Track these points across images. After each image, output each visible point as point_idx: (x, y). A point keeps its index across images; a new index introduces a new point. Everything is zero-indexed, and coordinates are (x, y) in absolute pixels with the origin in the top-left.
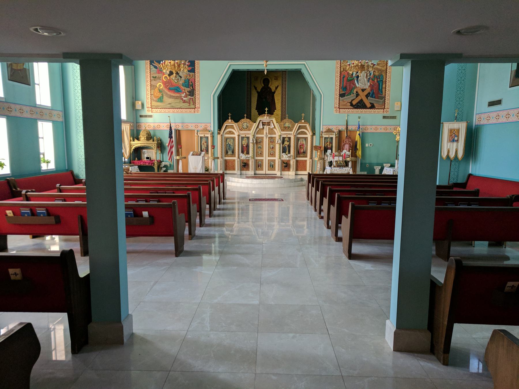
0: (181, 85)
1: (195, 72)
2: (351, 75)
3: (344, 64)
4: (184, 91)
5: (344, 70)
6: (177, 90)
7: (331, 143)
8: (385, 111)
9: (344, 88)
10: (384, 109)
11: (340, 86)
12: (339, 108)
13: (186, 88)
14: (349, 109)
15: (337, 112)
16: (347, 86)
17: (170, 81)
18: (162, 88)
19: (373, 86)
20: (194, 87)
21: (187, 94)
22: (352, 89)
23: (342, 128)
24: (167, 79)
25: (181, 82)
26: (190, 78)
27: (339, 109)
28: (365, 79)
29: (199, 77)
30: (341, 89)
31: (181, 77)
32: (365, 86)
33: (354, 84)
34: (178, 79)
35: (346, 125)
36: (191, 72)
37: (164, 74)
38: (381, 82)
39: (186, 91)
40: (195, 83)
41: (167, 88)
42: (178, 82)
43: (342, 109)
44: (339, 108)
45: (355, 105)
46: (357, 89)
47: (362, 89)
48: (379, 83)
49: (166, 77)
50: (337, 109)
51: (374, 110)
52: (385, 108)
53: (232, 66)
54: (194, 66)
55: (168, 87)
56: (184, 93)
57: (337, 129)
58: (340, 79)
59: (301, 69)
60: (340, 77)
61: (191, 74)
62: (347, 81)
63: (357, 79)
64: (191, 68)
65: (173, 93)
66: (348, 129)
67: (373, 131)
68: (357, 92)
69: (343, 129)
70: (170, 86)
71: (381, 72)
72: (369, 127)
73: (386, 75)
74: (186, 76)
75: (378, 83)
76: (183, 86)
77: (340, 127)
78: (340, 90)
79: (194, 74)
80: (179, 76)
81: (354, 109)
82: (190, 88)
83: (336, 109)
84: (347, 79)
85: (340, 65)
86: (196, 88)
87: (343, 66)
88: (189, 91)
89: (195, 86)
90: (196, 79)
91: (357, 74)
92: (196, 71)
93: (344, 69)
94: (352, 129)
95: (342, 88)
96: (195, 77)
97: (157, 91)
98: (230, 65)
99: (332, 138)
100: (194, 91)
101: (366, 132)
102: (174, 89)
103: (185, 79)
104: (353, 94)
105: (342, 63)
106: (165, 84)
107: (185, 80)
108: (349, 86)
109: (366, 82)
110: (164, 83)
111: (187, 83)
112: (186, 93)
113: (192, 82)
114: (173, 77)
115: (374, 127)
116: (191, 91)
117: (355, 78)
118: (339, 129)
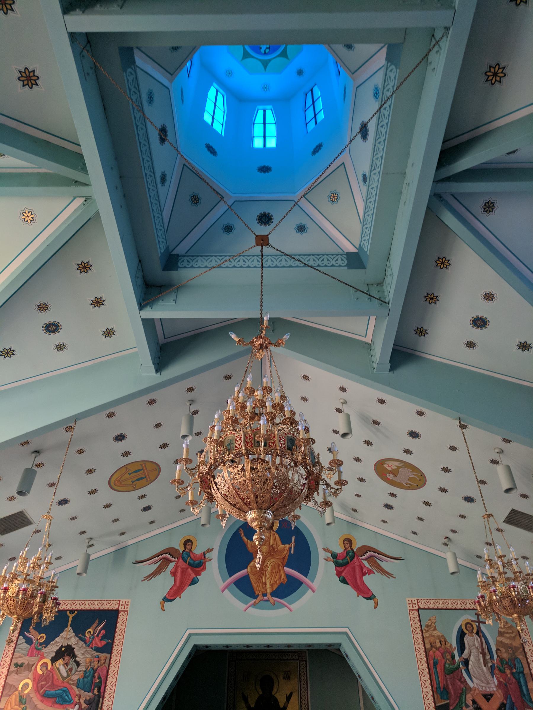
0: (73, 684)
1: (111, 653)
2: (451, 659)
3: (430, 632)
4: (77, 699)
5: (432, 646)
6: (60, 696)
9: (442, 692)
11: (431, 684)
13: (83, 691)
16: (447, 684)
17: (51, 675)
18: (28, 694)
19: (506, 686)
20: (102, 690)
21: (83, 707)
22: (462, 694)
24: (47, 668)
25: (75, 677)
26: (98, 667)
28: (484, 668)
29: (118, 663)
30: (437, 693)
31: (78, 664)
32: (489, 686)
33: (462, 680)
34: (71, 670)
36: (103, 653)
37: (42, 657)
38: (521, 675)
39: (82, 701)
40: (107, 680)
41: (39, 692)
42: (68, 676)
46: (472, 692)
47: (483, 693)
48: (518, 677)
49: (45, 664)
53: (192, 637)
54: (114, 637)
55: (42, 690)
56: (77, 706)
58: (428, 667)
59: (340, 645)
60: (427, 662)
61: (103, 655)
62: (445, 674)
63: (465, 668)
64: (104, 642)
65: (51, 706)
68: (474, 702)
70: (48, 687)
71: (514, 653)
73: (527, 659)
74: (91, 663)
75: (515, 678)
76: (78, 687)
78: (433, 695)
79: (108, 655)
80: (75, 661)
82: (93, 693)
84: (445, 668)
85: (422, 635)
86: (108, 691)
87: (427, 637)
88: (89, 700)
89: (106, 685)
90: (112, 668)
91: (463, 656)
92: (113, 651)
93: (432, 644)
95: (439, 692)
96: (110, 663)
97: (15, 700)
98: (190, 636)
100: (101, 699)
102: (56, 694)
103: (86, 669)
104: (467, 706)
105: (424, 631)
106: (38, 683)
107: (85, 672)
108: (453, 684)
109: (487, 675)
110: (37, 680)
111: (89, 678)
112: (79, 704)
113: (99, 677)
114: (60, 665)
116: (94, 698)
117: (461, 666)
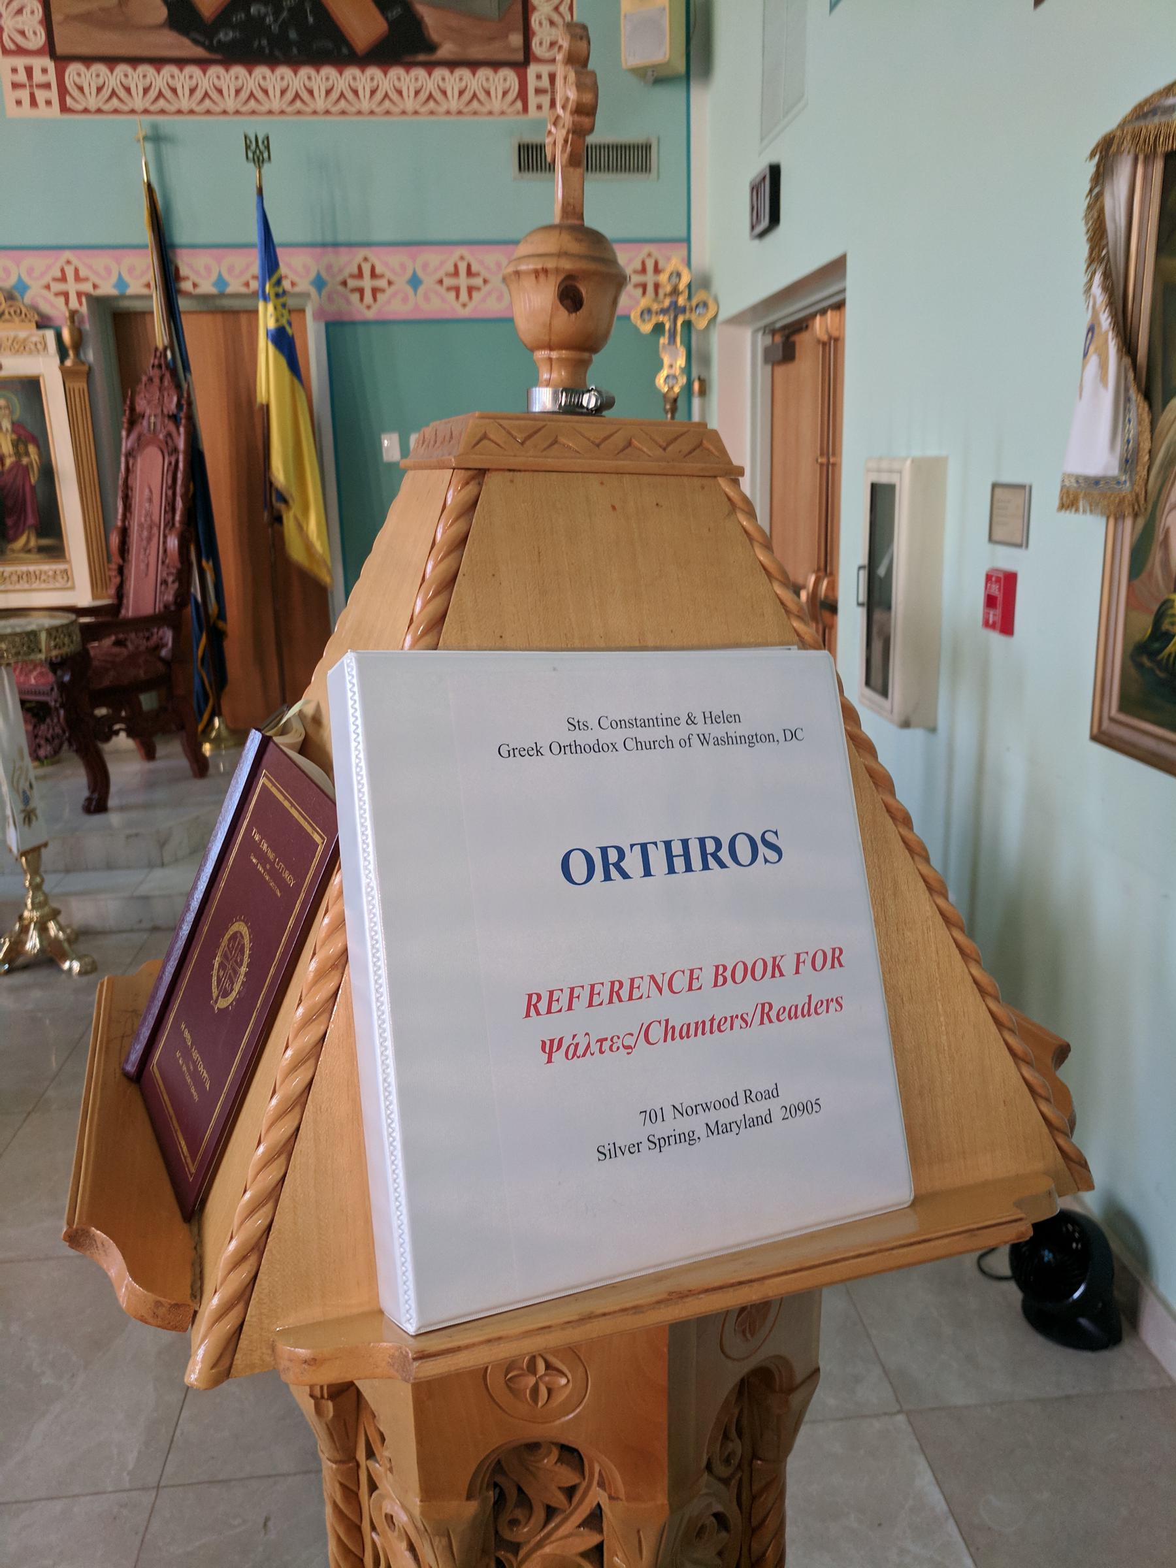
7: (34, 440)
8: (532, 83)
10: (521, 65)
12: (50, 49)
14: (158, 62)
15: (41, 95)
23: (121, 283)
27: (50, 65)
35: (146, 236)
43: (88, 60)
44: (50, 49)
45: (223, 18)
50: (29, 71)
51: (421, 72)
52: (528, 57)
57: (72, 287)
66: (186, 286)
67: (441, 304)
69: (135, 287)
72: (389, 262)
77: (101, 261)
81: (215, 70)
83: (20, 62)
94: (221, 282)
99: (31, 387)
101: (370, 315)
115: (436, 262)
118: (87, 287)
